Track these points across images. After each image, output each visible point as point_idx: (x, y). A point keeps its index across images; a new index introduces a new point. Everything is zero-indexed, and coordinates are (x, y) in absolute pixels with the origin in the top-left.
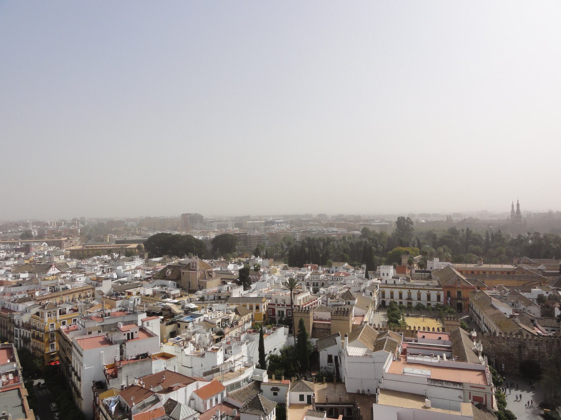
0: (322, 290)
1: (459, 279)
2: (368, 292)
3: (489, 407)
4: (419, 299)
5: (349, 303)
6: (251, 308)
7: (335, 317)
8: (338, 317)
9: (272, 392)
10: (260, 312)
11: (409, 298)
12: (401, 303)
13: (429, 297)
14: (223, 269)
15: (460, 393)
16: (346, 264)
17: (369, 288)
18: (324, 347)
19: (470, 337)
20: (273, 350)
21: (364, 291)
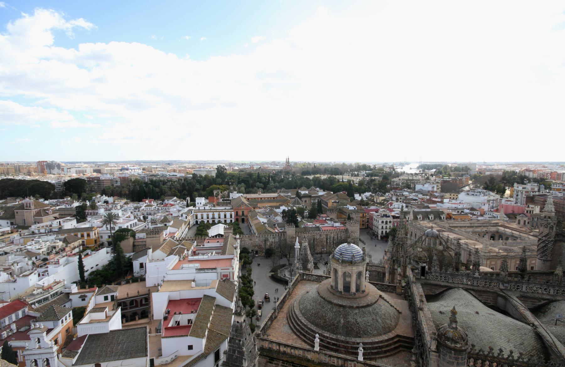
0: (150, 217)
1: (243, 203)
2: (184, 216)
3: (231, 280)
4: (219, 218)
5: (166, 225)
6: (82, 236)
7: (149, 236)
8: (152, 236)
9: (81, 299)
10: (91, 238)
11: (213, 218)
12: (208, 221)
13: (225, 216)
14: (68, 207)
15: (215, 274)
16: (175, 198)
17: (185, 213)
18: (136, 258)
19: (235, 238)
20: (94, 266)
21: (182, 216)
